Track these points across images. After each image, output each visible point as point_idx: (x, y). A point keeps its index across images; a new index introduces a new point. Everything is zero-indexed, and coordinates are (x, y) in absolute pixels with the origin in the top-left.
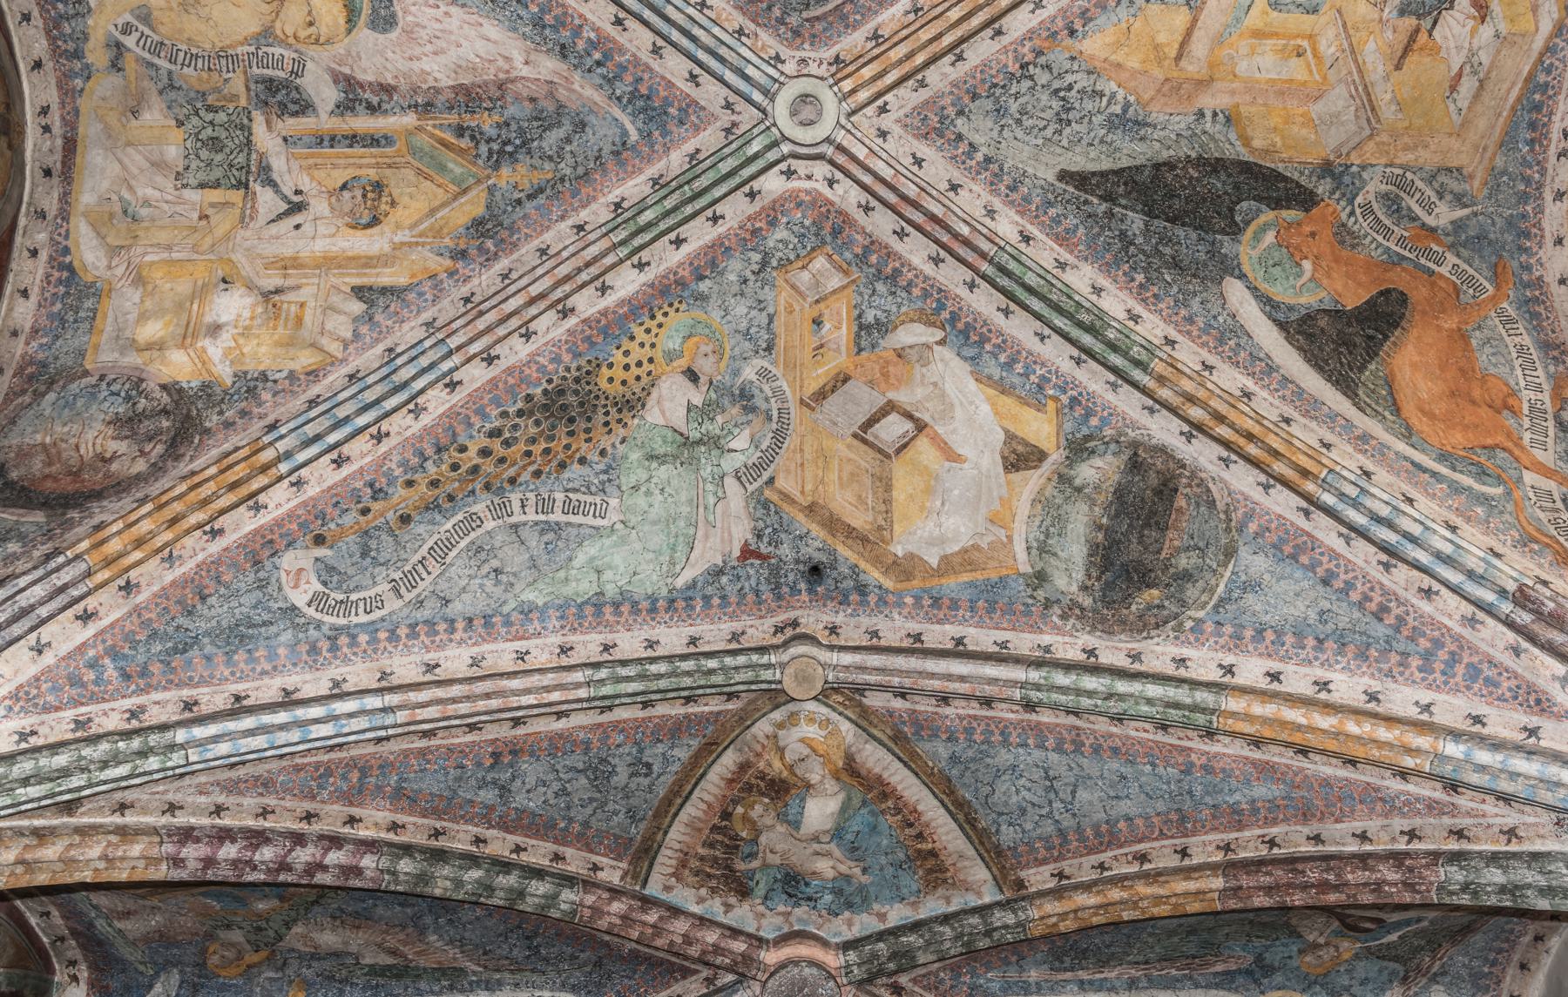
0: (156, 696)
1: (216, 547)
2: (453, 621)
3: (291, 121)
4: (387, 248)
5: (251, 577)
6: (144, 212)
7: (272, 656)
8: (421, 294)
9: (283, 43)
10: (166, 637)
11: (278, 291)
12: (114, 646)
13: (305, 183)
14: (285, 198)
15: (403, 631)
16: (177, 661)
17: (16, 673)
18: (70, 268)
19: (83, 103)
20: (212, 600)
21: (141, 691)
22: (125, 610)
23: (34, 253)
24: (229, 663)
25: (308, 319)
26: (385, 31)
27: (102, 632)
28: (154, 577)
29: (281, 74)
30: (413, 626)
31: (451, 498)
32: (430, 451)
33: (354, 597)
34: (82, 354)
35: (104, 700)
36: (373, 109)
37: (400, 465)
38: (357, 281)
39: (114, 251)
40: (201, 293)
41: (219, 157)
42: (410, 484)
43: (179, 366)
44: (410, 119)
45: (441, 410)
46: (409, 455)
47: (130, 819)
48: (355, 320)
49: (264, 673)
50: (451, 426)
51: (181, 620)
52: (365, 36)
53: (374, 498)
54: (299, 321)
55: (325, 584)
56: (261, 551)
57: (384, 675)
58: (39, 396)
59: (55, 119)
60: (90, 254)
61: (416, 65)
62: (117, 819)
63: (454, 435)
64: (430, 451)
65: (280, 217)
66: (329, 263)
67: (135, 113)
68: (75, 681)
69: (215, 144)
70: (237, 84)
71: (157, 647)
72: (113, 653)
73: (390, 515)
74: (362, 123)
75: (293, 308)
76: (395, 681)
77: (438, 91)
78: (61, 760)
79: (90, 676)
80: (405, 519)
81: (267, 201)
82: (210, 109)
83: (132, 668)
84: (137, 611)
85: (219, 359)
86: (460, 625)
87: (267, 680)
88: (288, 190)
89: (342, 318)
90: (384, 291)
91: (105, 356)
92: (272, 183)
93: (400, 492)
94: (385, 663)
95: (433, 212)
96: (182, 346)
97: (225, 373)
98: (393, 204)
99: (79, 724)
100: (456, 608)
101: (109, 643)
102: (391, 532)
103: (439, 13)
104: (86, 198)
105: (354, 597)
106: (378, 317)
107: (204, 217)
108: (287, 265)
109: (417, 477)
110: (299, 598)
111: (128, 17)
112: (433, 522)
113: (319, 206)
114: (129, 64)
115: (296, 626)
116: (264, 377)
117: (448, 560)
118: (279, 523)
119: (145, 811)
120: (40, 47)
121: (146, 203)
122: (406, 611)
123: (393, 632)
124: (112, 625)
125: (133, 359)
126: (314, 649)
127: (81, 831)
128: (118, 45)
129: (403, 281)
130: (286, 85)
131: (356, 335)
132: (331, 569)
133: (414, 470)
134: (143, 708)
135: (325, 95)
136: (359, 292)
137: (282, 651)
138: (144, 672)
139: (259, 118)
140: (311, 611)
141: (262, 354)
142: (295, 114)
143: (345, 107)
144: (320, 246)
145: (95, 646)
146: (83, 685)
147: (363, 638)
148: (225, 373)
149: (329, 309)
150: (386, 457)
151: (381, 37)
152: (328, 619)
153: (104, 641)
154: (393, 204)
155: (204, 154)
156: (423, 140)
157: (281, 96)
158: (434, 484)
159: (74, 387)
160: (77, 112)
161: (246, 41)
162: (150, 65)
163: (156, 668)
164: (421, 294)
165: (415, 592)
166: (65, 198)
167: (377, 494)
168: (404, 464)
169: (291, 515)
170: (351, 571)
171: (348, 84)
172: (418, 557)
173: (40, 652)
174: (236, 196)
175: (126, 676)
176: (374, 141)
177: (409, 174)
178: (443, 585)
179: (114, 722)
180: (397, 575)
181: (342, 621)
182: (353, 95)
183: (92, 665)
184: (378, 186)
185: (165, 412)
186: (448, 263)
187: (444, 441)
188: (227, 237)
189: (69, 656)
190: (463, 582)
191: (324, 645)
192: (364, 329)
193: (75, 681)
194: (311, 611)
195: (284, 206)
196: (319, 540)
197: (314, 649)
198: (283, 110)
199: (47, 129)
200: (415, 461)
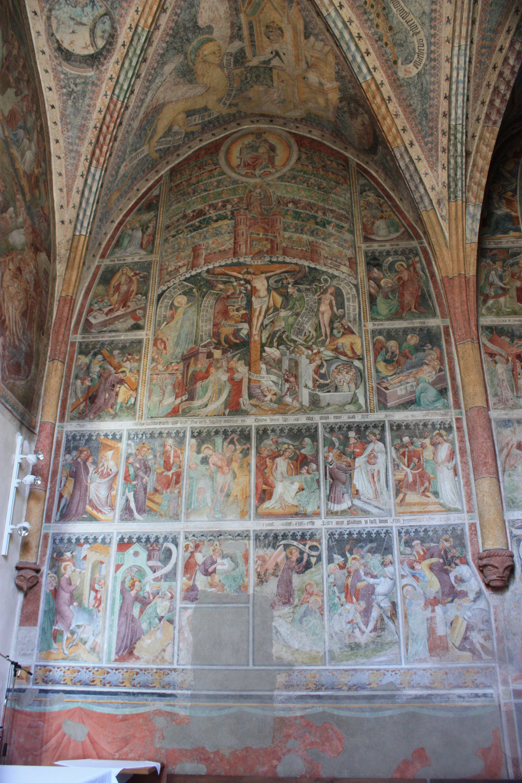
0: (439, 126)
1: (394, 99)
2: (432, 10)
3: (247, 55)
4: (290, 26)
5: (405, 88)
6: (282, 97)
7: (433, 83)
8: (307, 16)
9: (222, 60)
10: (421, 120)
11: (307, 63)
13: (269, 50)
14: (274, 57)
15: (432, 32)
16: (430, 117)
18: (302, 120)
19: (249, 112)
20: (412, 102)
23: (297, 127)
24: (433, 99)
25: (317, 55)
26: (213, 29)
28: (401, 121)
29: (232, 60)
30: (431, 27)
31: (384, 9)
32: (366, 17)
33: (417, 51)
34: (329, 121)
36: (240, 29)
37: (370, 29)
38: (303, 37)
39: (295, 107)
40: (309, 86)
41: (262, 75)
42: (377, 26)
43: (334, 97)
44: (242, 16)
45: (350, 12)
46: (367, 26)
47: (478, 134)
48: (317, 40)
49: (439, 87)
50: (357, 7)
51: (417, 114)
52: (216, 34)
53: (382, 40)
54: (317, 58)
55: (411, 62)
56: (397, 83)
57: (448, 41)
58: (342, 134)
59: (255, 119)
60: (297, 114)
61: (223, 16)
62: (477, 138)
63: (360, 6)
64: (366, 17)
65: (281, 59)
66: (296, 45)
67: (250, 99)
68: (430, 150)
69: (258, 77)
70: (238, 71)
71: (424, 123)
72: (423, 137)
73: (389, 34)
74: (245, 32)
75: (313, 59)
76: (451, 36)
77: (230, 7)
78: (452, 161)
79: (430, 145)
80: (391, 28)
81: (275, 62)
82: (246, 78)
83: (430, 132)
84: (412, 128)
85: (331, 85)
86: (434, 7)
87: (442, 86)
88: (271, 56)
89: (316, 44)
90: (306, 28)
91: (330, 115)
92: (270, 60)
93: (380, 30)
94: (443, 40)
95: (276, 9)
96: (327, 94)
97: (336, 84)
98: (273, 22)
99: (444, 151)
100: (427, 9)
102: (395, 35)
103: (203, 11)
104: (279, 112)
105: (417, 51)
106: (316, 32)
107: (283, 81)
108: (298, 59)
109: (375, 22)
110: (415, 71)
111: (221, 104)
112: (393, 17)
113: (276, 46)
114: (235, 102)
115: (424, 74)
116: (337, 73)
117: (408, 11)
118: (388, 77)
119: (476, 129)
120: (233, 124)
121: (279, 96)
122: (425, 30)
123: (432, 36)
124: (415, 137)
125: (331, 108)
126: (434, 68)
127: (477, 152)
128: (230, 105)
129: (302, 22)
130: (236, 58)
131: (322, 40)
132: (406, 59)
133: (372, 24)
134: (443, 131)
135: (237, 45)
136: (307, 37)
137: (432, 80)
138: (431, 128)
139: (247, 64)
140: (420, 68)
141: (330, 71)
142: (245, 54)
143: (240, 38)
144: (290, 47)
147: (433, 48)
148: (336, 84)
149: (313, 47)
150: (367, 35)
151: (215, 30)
152: (423, 62)
154: (273, 22)
155: (261, 80)
156: (249, 10)
157: (239, 58)
158: (378, 16)
159: (340, 125)
160: (252, 114)
161: (223, 71)
162: (234, 96)
163: (431, 124)
164: (307, 16)
165: (419, 26)
166: (280, 117)
167: (380, 39)
168: (370, 28)
169: (385, 72)
170: (408, 51)
171: (232, 38)
172: (405, 24)
174: (275, 71)
175: (432, 135)
176: (251, 27)
177: (262, 16)
178: (417, 14)
179: (445, 140)
180: (411, 33)
181: (425, 56)
182: (236, 34)
184: (267, 27)
185: (349, 104)
186: (294, 4)
187: (362, 11)
188: (289, 76)
189: (423, 151)
190: (417, 5)
191: (433, 63)
192: (320, 38)
194: (420, 68)
195: (277, 58)
196: (395, 62)
197: (434, 68)
198: (244, 57)
199: (258, 121)
200: (369, 23)
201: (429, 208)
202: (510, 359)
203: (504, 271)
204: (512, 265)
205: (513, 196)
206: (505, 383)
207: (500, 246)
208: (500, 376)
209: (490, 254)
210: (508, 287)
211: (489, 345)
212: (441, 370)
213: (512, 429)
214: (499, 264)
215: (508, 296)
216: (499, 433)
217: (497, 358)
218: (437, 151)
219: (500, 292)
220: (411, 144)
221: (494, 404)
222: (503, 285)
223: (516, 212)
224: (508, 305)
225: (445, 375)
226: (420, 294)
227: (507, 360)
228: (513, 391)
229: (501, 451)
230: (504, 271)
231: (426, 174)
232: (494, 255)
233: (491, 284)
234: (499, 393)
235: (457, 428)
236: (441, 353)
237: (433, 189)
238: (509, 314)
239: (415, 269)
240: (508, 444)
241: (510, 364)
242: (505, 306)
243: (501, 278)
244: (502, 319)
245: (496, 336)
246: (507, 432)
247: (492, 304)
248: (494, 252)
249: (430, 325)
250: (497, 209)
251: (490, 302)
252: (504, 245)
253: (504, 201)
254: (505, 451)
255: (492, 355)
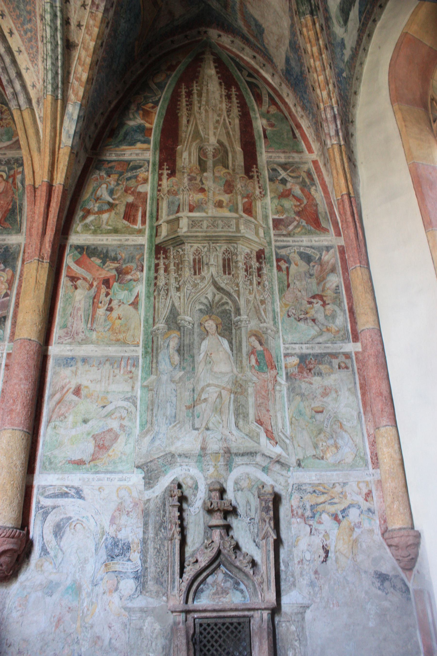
12: (21, 24)
17: (26, 61)
21: (35, 16)
22: (9, 17)
27: (16, 28)
35: (37, 30)
68: (30, 40)
72: (23, 24)
79: (29, 33)
101: (20, 25)
124: (14, 23)
145: (20, 31)
146: (32, 37)
153: (19, 27)
173: (21, 51)
175: (30, 21)
183: (26, 33)
189: (23, 41)
193: (31, 39)
201: (24, 107)
202: (95, 284)
203: (118, 184)
204: (129, 179)
205: (153, 107)
206: (81, 313)
207: (121, 158)
208: (77, 305)
209: (106, 166)
210: (117, 202)
211: (74, 267)
212: (6, 295)
213: (74, 368)
214: (114, 177)
215: (113, 213)
216: (55, 373)
217: (79, 282)
218: (37, 41)
219: (106, 207)
220: (11, 33)
221: (60, 337)
222: (111, 200)
223: (151, 124)
224: (110, 223)
225: (9, 301)
226: (10, 207)
227: (91, 285)
228: (87, 322)
229: (52, 395)
230: (118, 184)
231: (27, 69)
232: (111, 168)
233: (97, 199)
234: (69, 324)
235: (6, 365)
236: (13, 276)
237: (34, 86)
238: (109, 232)
239: (14, 179)
240: (63, 388)
241: (93, 291)
242: (107, 223)
243: (111, 193)
244: (99, 237)
245: (86, 256)
246: (66, 372)
247: (92, 222)
248: (113, 164)
249: (10, 242)
250: (130, 119)
251: (91, 218)
252: (127, 157)
253: (141, 112)
254: (58, 397)
255: (73, 279)
